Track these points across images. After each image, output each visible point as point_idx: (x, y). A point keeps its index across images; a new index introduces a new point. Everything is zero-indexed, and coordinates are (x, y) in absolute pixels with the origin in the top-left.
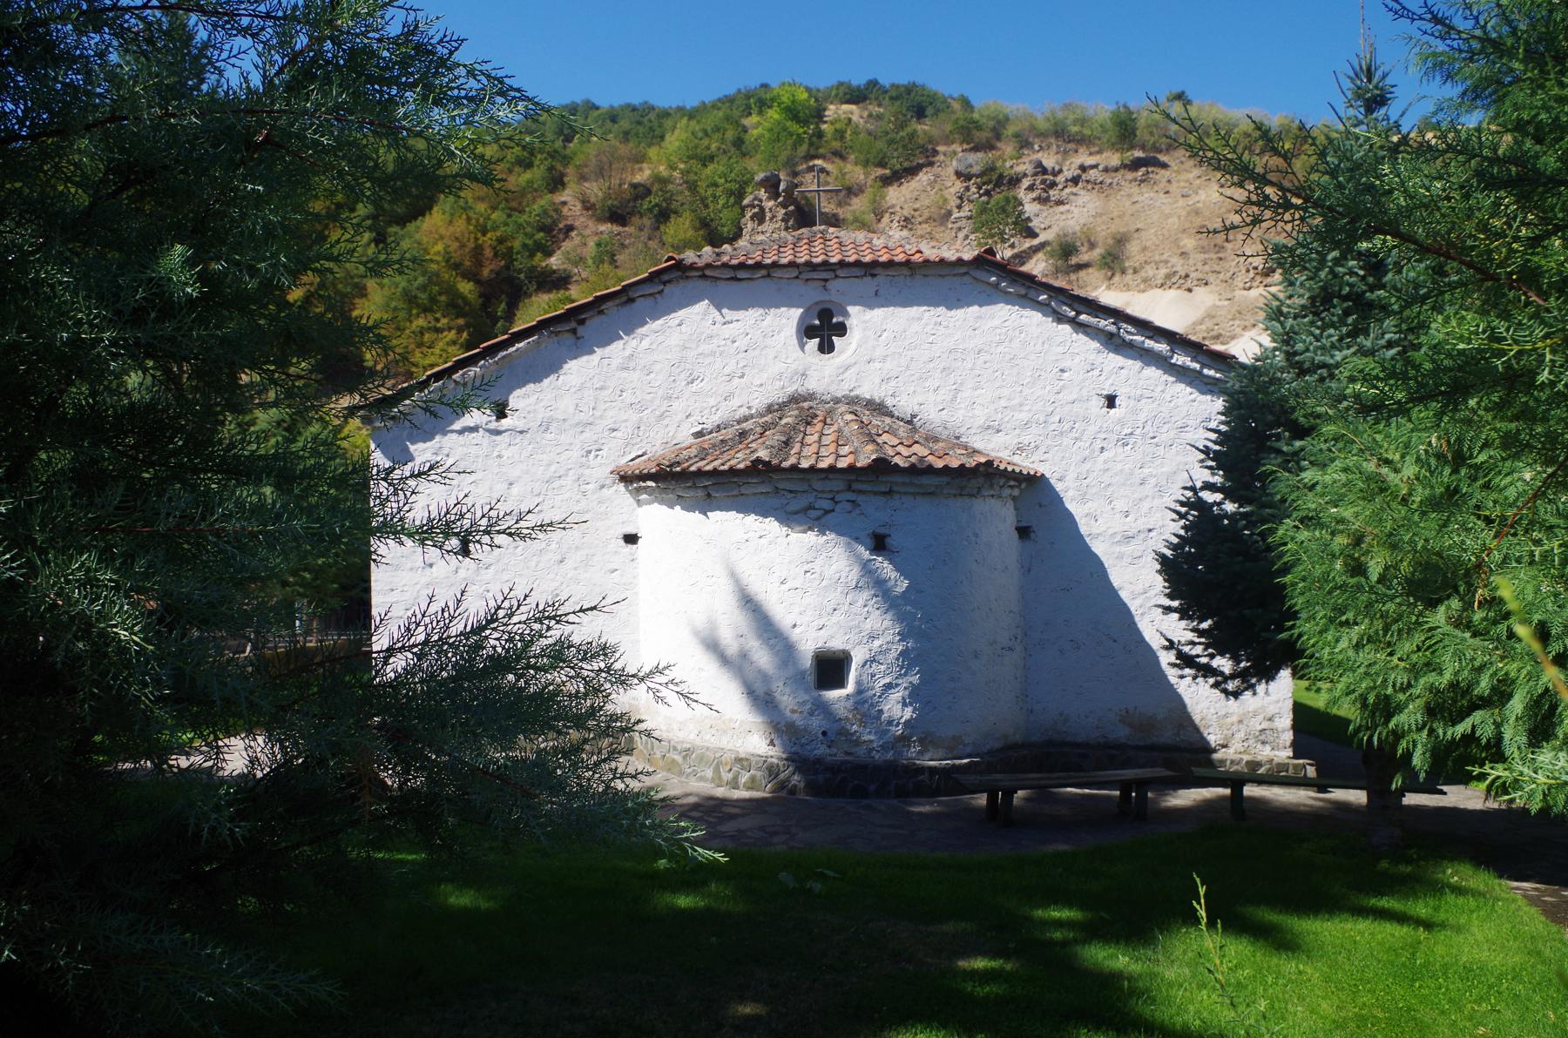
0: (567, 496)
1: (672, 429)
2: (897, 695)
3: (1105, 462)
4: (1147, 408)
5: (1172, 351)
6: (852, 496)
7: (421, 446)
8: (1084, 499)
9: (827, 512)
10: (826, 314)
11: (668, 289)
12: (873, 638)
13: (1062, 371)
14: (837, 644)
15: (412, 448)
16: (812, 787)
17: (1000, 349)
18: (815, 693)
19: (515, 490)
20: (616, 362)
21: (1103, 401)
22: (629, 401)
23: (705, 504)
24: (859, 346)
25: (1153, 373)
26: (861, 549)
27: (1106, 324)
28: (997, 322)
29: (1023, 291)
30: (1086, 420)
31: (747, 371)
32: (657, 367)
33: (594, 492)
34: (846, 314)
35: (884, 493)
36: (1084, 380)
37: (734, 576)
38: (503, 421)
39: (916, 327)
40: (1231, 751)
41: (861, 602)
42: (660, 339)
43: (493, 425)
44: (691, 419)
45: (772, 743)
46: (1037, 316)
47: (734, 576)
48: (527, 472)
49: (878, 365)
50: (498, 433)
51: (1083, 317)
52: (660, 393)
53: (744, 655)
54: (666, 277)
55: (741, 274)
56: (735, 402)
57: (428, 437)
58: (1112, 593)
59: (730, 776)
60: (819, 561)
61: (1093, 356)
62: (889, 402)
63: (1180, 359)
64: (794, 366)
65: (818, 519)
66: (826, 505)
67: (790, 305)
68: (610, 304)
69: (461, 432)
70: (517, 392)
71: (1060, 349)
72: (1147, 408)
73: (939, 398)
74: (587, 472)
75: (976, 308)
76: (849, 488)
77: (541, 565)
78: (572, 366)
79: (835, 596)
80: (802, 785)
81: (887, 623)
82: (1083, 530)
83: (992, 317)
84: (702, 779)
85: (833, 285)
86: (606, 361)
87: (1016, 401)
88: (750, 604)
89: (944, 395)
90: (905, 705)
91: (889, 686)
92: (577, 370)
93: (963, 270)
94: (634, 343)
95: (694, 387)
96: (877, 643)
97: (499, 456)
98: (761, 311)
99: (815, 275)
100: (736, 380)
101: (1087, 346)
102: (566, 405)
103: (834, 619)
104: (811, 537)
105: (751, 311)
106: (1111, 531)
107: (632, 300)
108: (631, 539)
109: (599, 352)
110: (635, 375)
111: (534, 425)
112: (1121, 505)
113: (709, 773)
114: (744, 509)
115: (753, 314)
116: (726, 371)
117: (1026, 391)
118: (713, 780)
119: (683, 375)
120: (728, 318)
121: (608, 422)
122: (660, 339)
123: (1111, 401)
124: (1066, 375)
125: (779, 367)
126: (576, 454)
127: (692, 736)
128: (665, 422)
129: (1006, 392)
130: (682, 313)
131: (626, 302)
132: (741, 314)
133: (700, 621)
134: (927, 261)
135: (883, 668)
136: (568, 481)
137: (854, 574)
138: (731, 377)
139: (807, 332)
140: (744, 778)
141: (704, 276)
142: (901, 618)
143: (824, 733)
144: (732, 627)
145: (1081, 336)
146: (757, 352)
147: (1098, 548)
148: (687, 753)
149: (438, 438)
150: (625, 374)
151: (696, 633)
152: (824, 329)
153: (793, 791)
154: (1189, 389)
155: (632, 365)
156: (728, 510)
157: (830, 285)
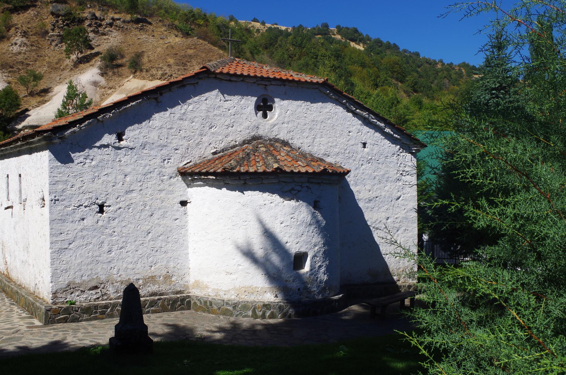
0: (154, 182)
1: (203, 150)
2: (323, 270)
3: (363, 170)
4: (376, 149)
5: (385, 127)
6: (308, 185)
7: (78, 154)
8: (356, 185)
9: (299, 191)
10: (265, 100)
11: (200, 82)
12: (315, 246)
13: (349, 132)
14: (303, 250)
15: (72, 155)
16: (297, 314)
17: (329, 122)
18: (295, 272)
19: (128, 179)
20: (177, 116)
21: (362, 145)
22: (183, 135)
23: (242, 189)
24: (279, 116)
25: (378, 135)
26: (311, 207)
27: (365, 114)
28: (328, 110)
29: (337, 98)
30: (357, 152)
31: (235, 124)
32: (196, 120)
33: (167, 180)
34: (274, 102)
35: (319, 183)
36: (357, 136)
37: (261, 222)
38: (122, 142)
39: (300, 110)
40: (400, 282)
41: (311, 232)
42: (198, 106)
43: (117, 145)
44: (211, 146)
45: (276, 296)
46: (341, 109)
47: (261, 222)
48: (134, 169)
49: (286, 125)
50: (119, 148)
51: (358, 110)
52: (198, 132)
53: (267, 258)
54: (201, 76)
55: (234, 79)
56: (230, 139)
57: (82, 150)
58: (365, 222)
59: (261, 313)
60: (296, 213)
61: (359, 127)
62: (290, 142)
63: (387, 130)
64: (254, 123)
65: (295, 195)
66: (298, 188)
67: (252, 96)
68: (176, 86)
69: (99, 147)
70: (130, 128)
71: (349, 123)
72: (376, 149)
73: (308, 141)
74: (164, 170)
75: (321, 103)
76: (308, 182)
77: (142, 217)
78: (156, 116)
79: (302, 228)
80: (293, 313)
81: (319, 239)
82: (356, 197)
83: (326, 108)
84: (246, 316)
85: (270, 88)
86: (172, 115)
87: (334, 144)
88: (269, 235)
89: (309, 140)
90: (325, 274)
91: (320, 267)
92: (159, 119)
93: (317, 86)
94: (185, 107)
95: (213, 130)
96: (316, 248)
97: (120, 161)
98: (240, 97)
99: (264, 83)
100: (230, 128)
101: (357, 122)
102: (154, 136)
103: (302, 239)
104: (293, 203)
105: (236, 97)
106: (365, 198)
107: (184, 86)
108: (184, 203)
109: (170, 110)
110: (186, 123)
111: (138, 145)
112: (368, 187)
113: (250, 313)
114: (263, 190)
115: (236, 98)
116: (226, 123)
117: (338, 140)
118: (252, 316)
119: (207, 124)
120: (227, 99)
121: (174, 145)
122: (198, 106)
123: (364, 145)
124: (351, 134)
125: (247, 124)
126: (158, 161)
127: (233, 297)
128: (200, 146)
129: (331, 140)
130: (207, 94)
131: (181, 87)
132: (232, 98)
133: (241, 241)
134: (293, 80)
135: (318, 258)
136: (155, 175)
137: (309, 218)
138: (228, 126)
139: (258, 108)
140: (268, 313)
141: (215, 78)
142: (324, 237)
143: (299, 289)
144: (259, 246)
145: (356, 118)
146: (239, 116)
147: (361, 205)
148: (235, 306)
149: (87, 151)
150: (181, 122)
151: (238, 248)
152: (264, 107)
153: (290, 316)
154: (389, 142)
155: (184, 118)
156: (254, 190)
157: (268, 88)
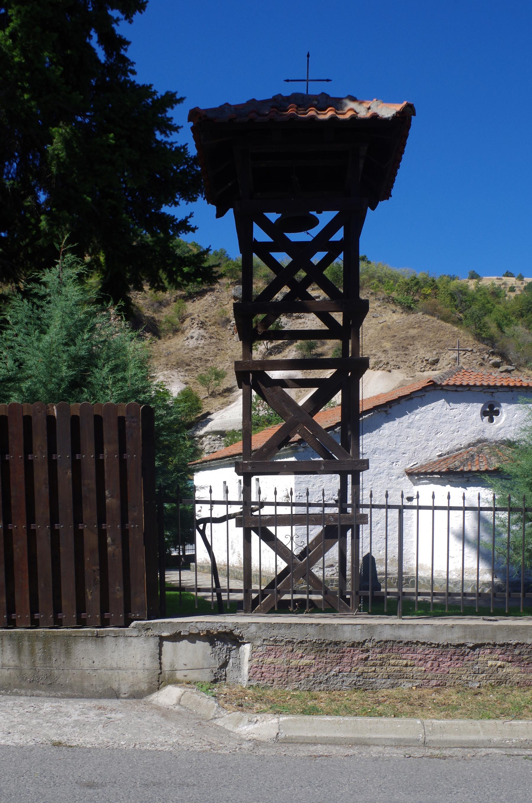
10: (491, 407)
11: (427, 394)
20: (405, 425)
24: (506, 420)
31: (460, 429)
34: (500, 406)
44: (437, 449)
52: (424, 438)
54: (428, 389)
55: (460, 389)
56: (455, 442)
68: (404, 400)
74: (392, 471)
78: (386, 425)
85: (496, 395)
86: (401, 424)
95: (438, 436)
98: (466, 404)
102: (383, 443)
107: (412, 399)
116: (452, 429)
121: (402, 450)
122: (425, 415)
125: (473, 428)
126: (387, 463)
128: (426, 450)
130: (433, 404)
132: (458, 405)
136: (383, 475)
138: (454, 432)
139: (484, 413)
141: (442, 389)
146: (465, 422)
150: (409, 430)
152: (490, 412)
155: (412, 426)
